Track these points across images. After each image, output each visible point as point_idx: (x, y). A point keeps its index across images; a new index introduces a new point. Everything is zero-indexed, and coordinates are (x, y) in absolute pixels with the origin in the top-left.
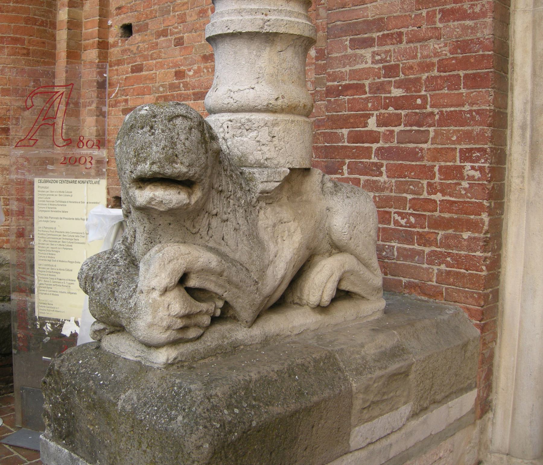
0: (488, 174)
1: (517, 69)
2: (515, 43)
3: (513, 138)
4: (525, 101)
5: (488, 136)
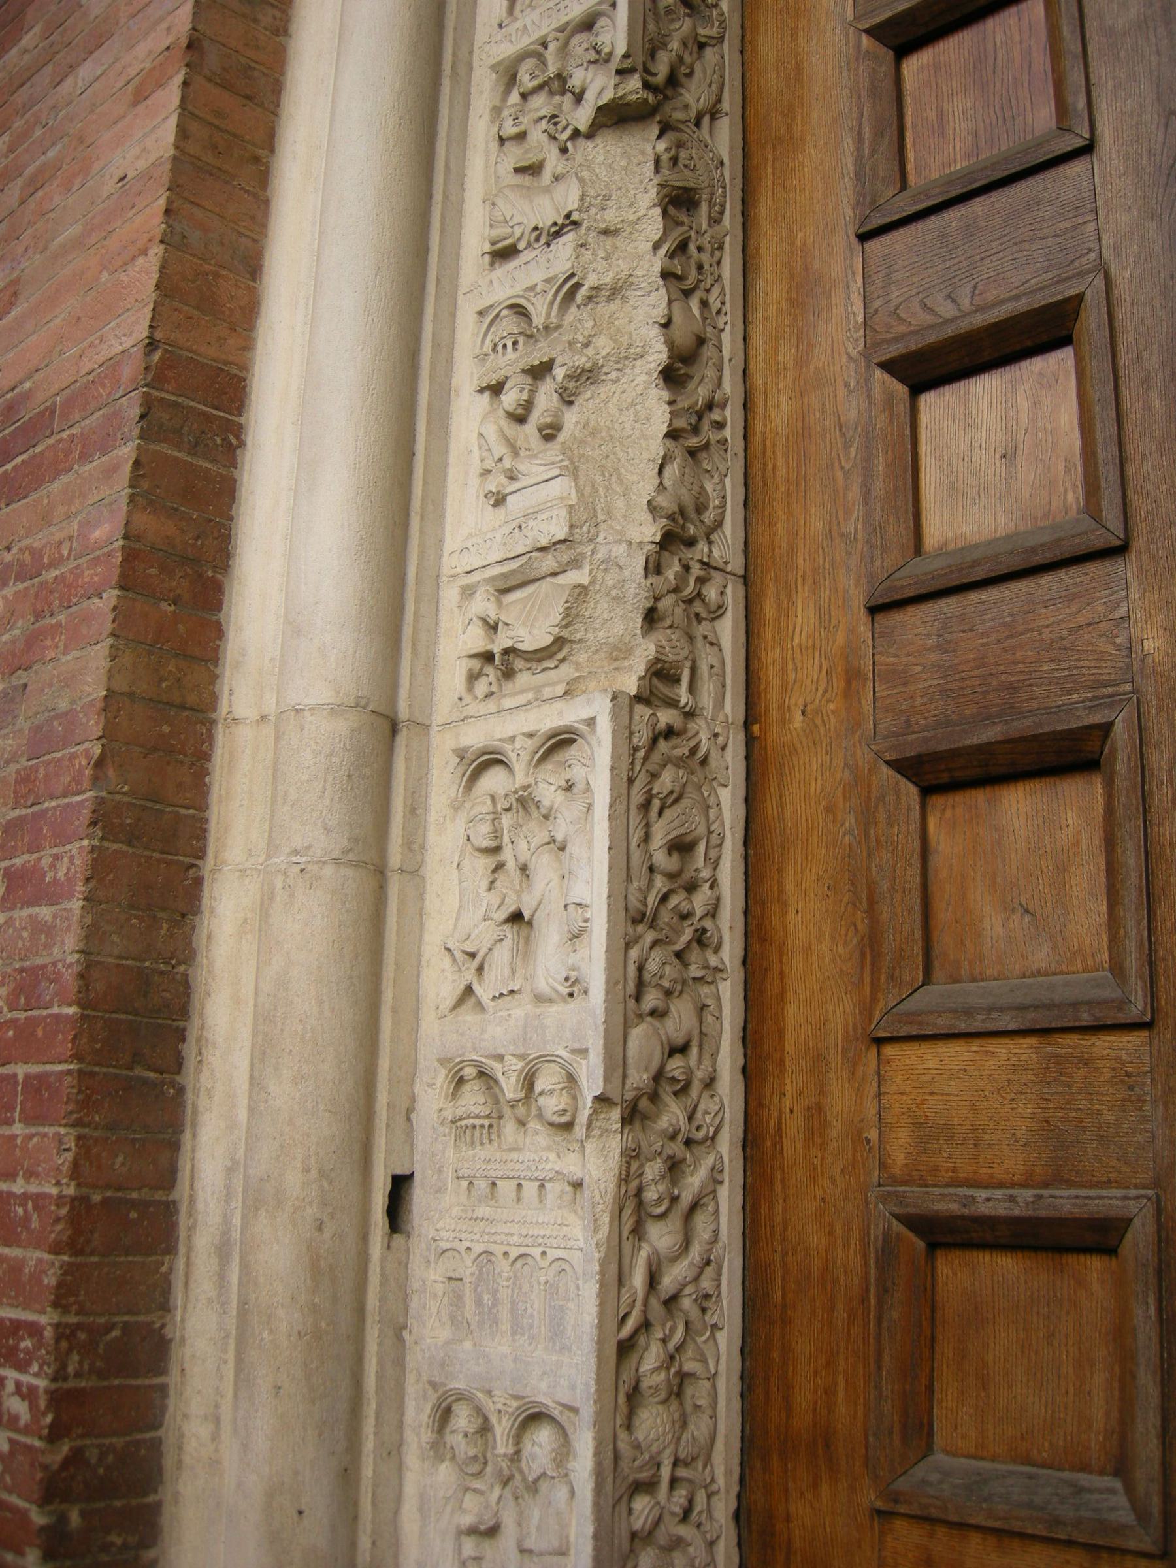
0: (44, 1414)
1: (214, 1059)
2: (209, 972)
3: (192, 1285)
4: (229, 1164)
5: (47, 1286)
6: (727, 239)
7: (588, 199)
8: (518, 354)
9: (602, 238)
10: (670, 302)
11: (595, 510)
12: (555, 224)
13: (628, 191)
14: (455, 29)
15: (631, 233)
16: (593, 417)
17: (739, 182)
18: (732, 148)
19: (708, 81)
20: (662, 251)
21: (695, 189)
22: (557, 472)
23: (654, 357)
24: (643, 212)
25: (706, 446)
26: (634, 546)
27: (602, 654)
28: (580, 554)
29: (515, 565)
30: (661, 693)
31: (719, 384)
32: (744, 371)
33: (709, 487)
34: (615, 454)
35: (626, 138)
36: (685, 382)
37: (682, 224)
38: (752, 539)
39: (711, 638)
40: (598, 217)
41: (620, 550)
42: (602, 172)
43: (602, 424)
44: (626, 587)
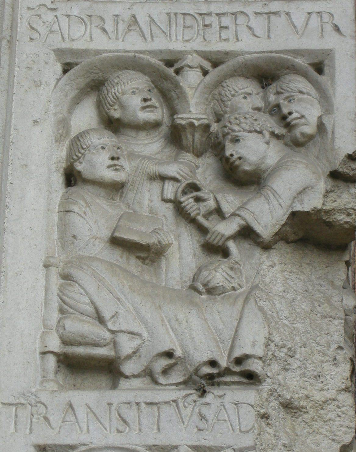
12: (213, 363)
15: (313, 419)
24: (331, 394)
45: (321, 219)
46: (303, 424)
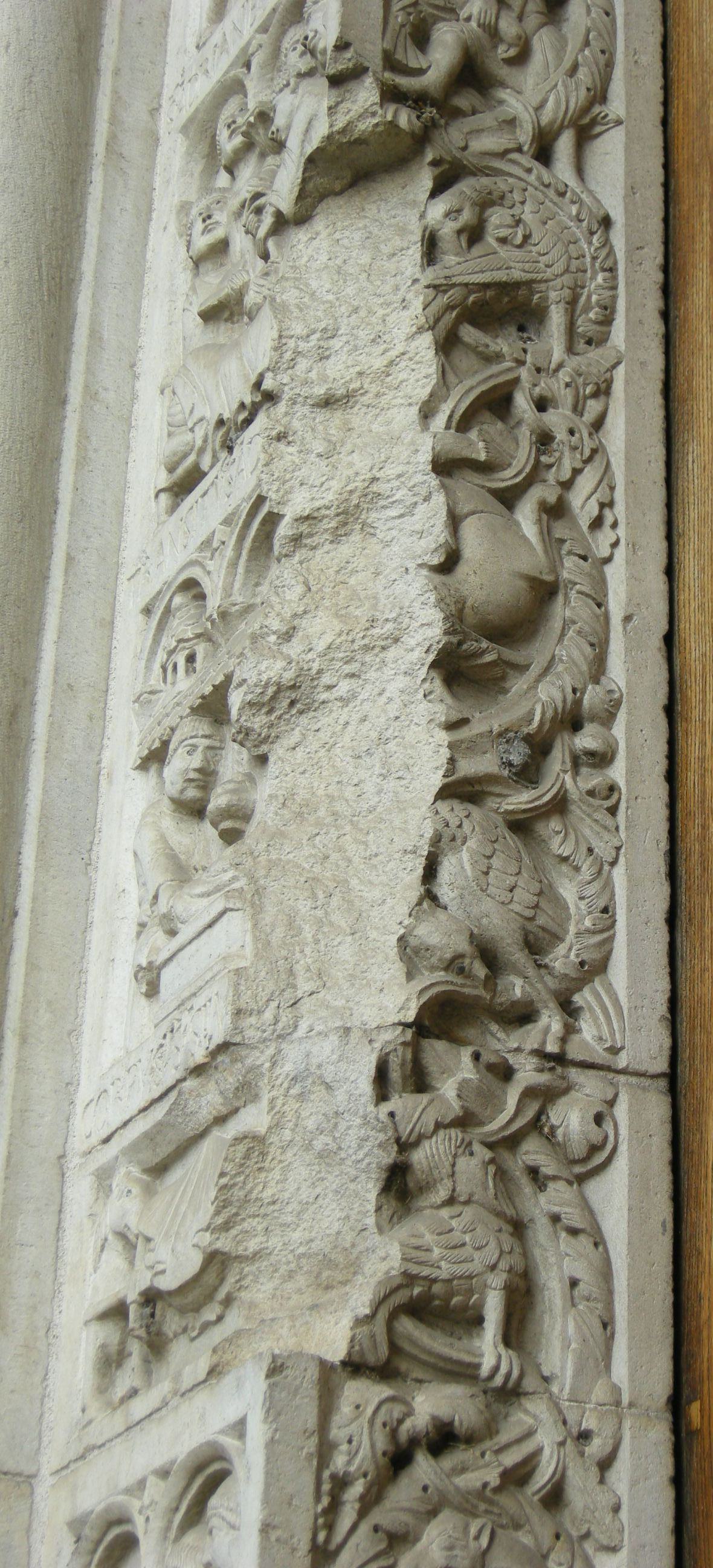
6: (620, 374)
7: (291, 343)
8: (193, 678)
9: (321, 415)
10: (454, 521)
11: (291, 972)
12: (242, 406)
13: (371, 312)
14: (117, 72)
16: (303, 781)
17: (654, 254)
18: (631, 190)
19: (567, 64)
20: (439, 421)
21: (529, 283)
22: (219, 906)
23: (419, 637)
24: (399, 348)
25: (560, 805)
26: (355, 1035)
27: (301, 1280)
28: (250, 1070)
29: (159, 1112)
30: (424, 1350)
31: (598, 668)
32: (669, 640)
33: (568, 891)
34: (340, 850)
35: (371, 209)
36: (503, 678)
37: (498, 357)
38: (684, 992)
39: (573, 1216)
40: (313, 375)
41: (326, 1049)
42: (322, 284)
43: (321, 792)
44: (342, 1126)
45: (342, 144)
46: (364, 410)
